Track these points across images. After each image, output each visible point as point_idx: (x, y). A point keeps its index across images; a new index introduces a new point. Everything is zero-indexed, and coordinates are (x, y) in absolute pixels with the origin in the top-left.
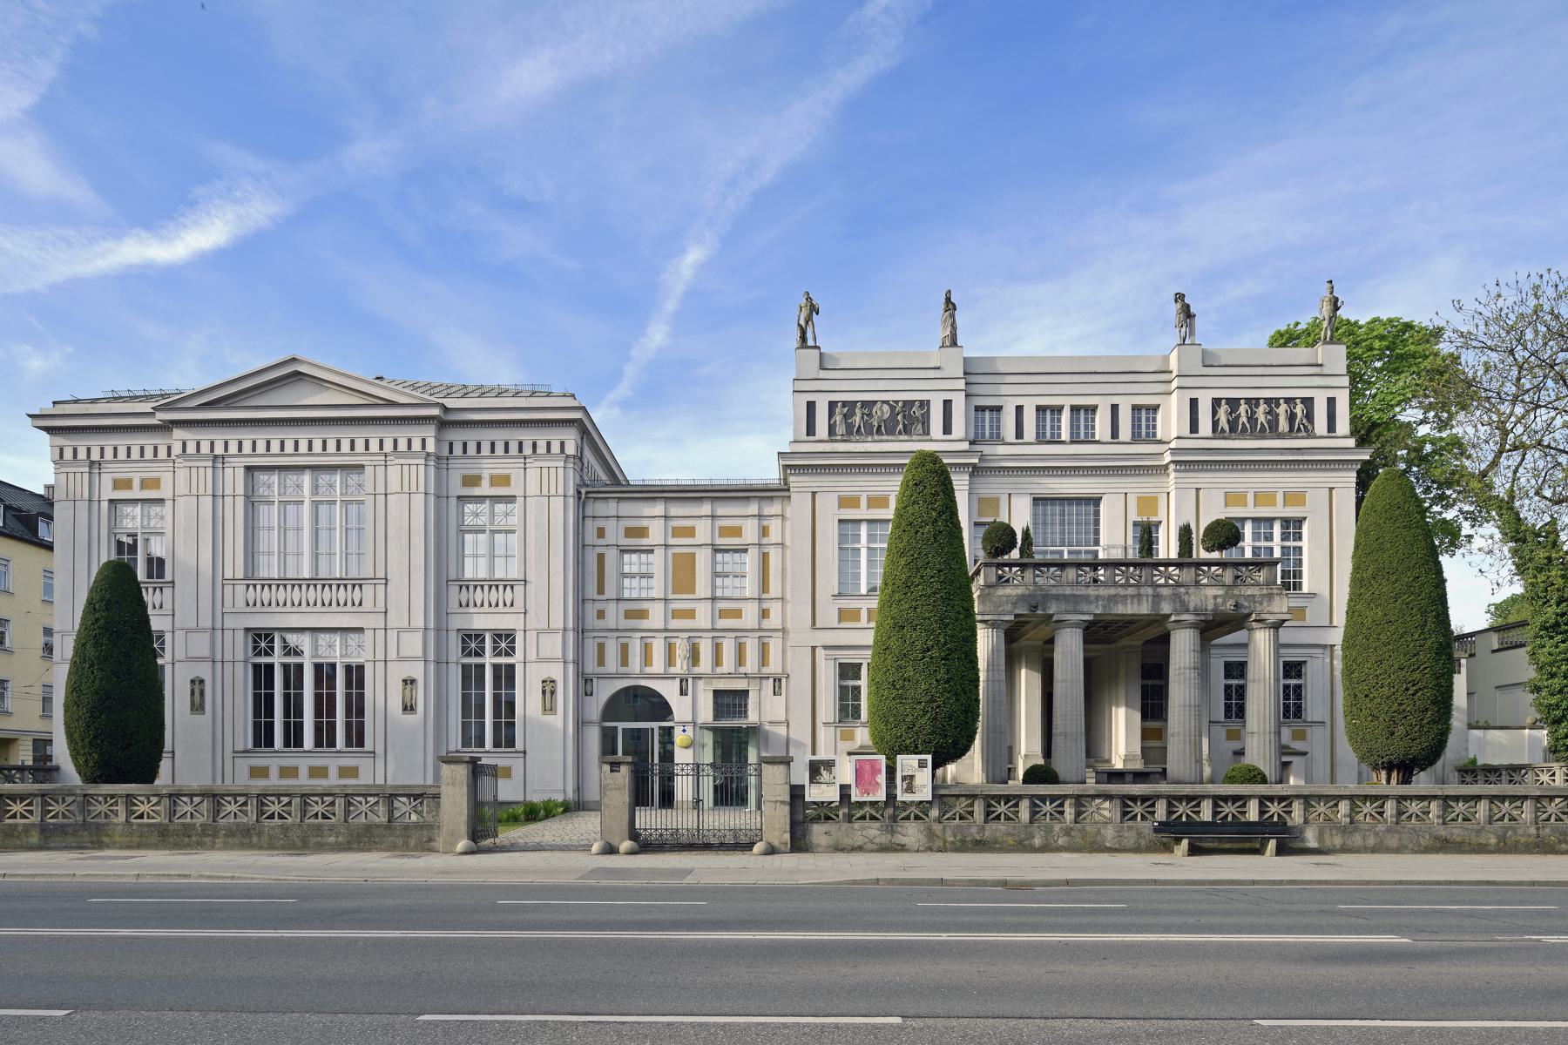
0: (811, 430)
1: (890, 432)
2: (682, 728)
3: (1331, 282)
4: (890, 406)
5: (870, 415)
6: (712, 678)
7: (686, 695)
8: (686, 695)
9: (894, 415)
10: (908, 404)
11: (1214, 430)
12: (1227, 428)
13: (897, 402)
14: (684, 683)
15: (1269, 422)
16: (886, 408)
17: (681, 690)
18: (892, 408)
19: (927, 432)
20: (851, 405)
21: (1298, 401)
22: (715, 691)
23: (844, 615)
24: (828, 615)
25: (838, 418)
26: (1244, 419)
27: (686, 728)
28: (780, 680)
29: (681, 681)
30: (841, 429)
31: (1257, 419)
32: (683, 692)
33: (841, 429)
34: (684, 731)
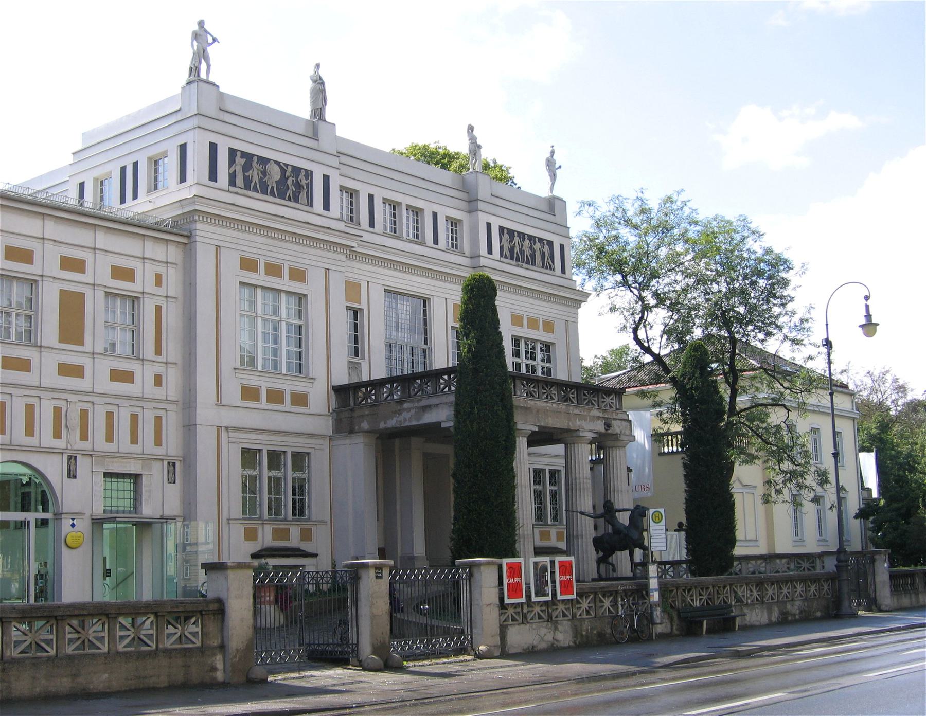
0: (213, 176)
1: (282, 196)
2: (71, 522)
3: (553, 146)
4: (281, 168)
5: (264, 173)
6: (105, 457)
7: (75, 477)
8: (75, 477)
9: (284, 178)
10: (296, 170)
11: (501, 256)
12: (508, 255)
13: (287, 165)
14: (73, 461)
15: (531, 255)
16: (276, 168)
17: (69, 470)
18: (283, 171)
19: (310, 203)
20: (248, 156)
21: (545, 242)
22: (104, 473)
23: (250, 393)
24: (232, 393)
25: (239, 169)
26: (517, 249)
27: (75, 522)
28: (174, 464)
29: (70, 458)
30: (240, 181)
31: (524, 251)
32: (72, 474)
33: (240, 181)
34: (73, 525)
